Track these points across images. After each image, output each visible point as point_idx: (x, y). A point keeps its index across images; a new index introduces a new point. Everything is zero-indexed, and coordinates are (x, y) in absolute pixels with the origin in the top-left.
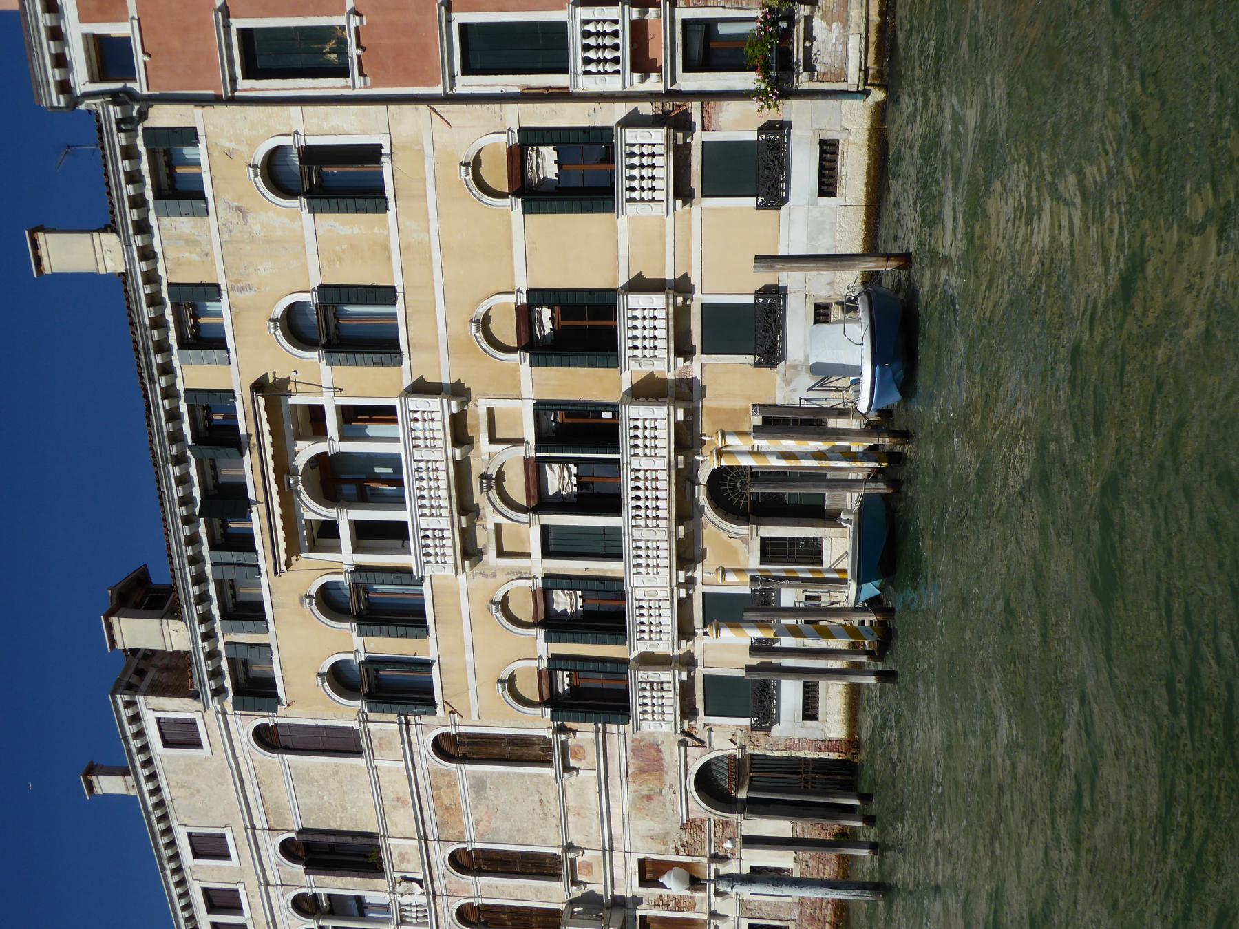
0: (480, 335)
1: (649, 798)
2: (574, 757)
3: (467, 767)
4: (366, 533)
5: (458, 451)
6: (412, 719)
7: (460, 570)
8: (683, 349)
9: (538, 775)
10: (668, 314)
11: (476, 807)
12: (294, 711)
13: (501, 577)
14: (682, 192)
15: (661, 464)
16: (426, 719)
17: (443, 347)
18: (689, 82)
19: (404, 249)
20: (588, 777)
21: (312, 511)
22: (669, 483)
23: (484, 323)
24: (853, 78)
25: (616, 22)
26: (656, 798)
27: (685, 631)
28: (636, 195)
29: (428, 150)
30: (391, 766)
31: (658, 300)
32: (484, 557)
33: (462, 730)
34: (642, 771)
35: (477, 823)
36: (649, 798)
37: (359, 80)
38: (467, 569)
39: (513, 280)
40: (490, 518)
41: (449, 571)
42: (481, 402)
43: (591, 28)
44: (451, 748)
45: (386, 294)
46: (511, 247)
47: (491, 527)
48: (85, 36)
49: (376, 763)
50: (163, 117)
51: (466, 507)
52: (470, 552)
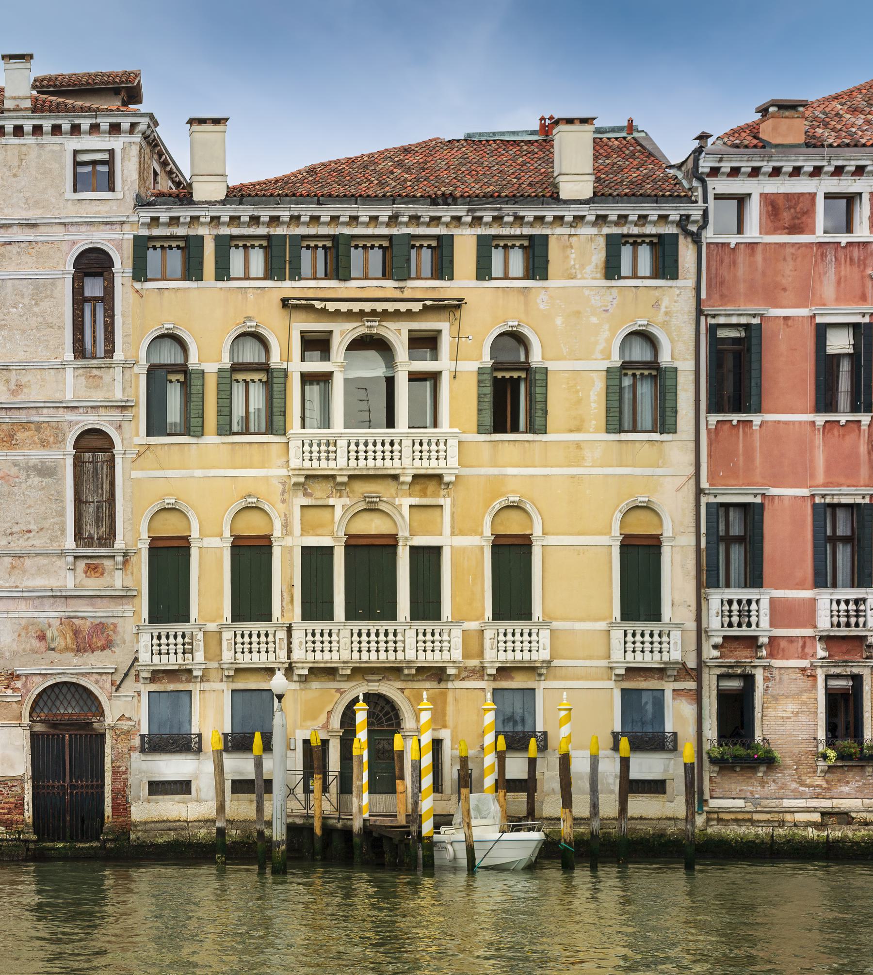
1: (42, 637)
2: (88, 566)
3: (70, 461)
8: (504, 671)
9: (63, 531)
10: (535, 661)
11: (15, 465)
12: (132, 297)
14: (632, 672)
15: (411, 655)
19: (578, 445)
20: (68, 580)
22: (394, 662)
25: (757, 625)
26: (43, 645)
28: (630, 638)
29: (659, 471)
30: (70, 385)
33: (118, 461)
34: (76, 632)
36: (42, 637)
43: (754, 606)
44: (94, 445)
47: (331, 501)
49: (69, 371)
50: (687, 254)
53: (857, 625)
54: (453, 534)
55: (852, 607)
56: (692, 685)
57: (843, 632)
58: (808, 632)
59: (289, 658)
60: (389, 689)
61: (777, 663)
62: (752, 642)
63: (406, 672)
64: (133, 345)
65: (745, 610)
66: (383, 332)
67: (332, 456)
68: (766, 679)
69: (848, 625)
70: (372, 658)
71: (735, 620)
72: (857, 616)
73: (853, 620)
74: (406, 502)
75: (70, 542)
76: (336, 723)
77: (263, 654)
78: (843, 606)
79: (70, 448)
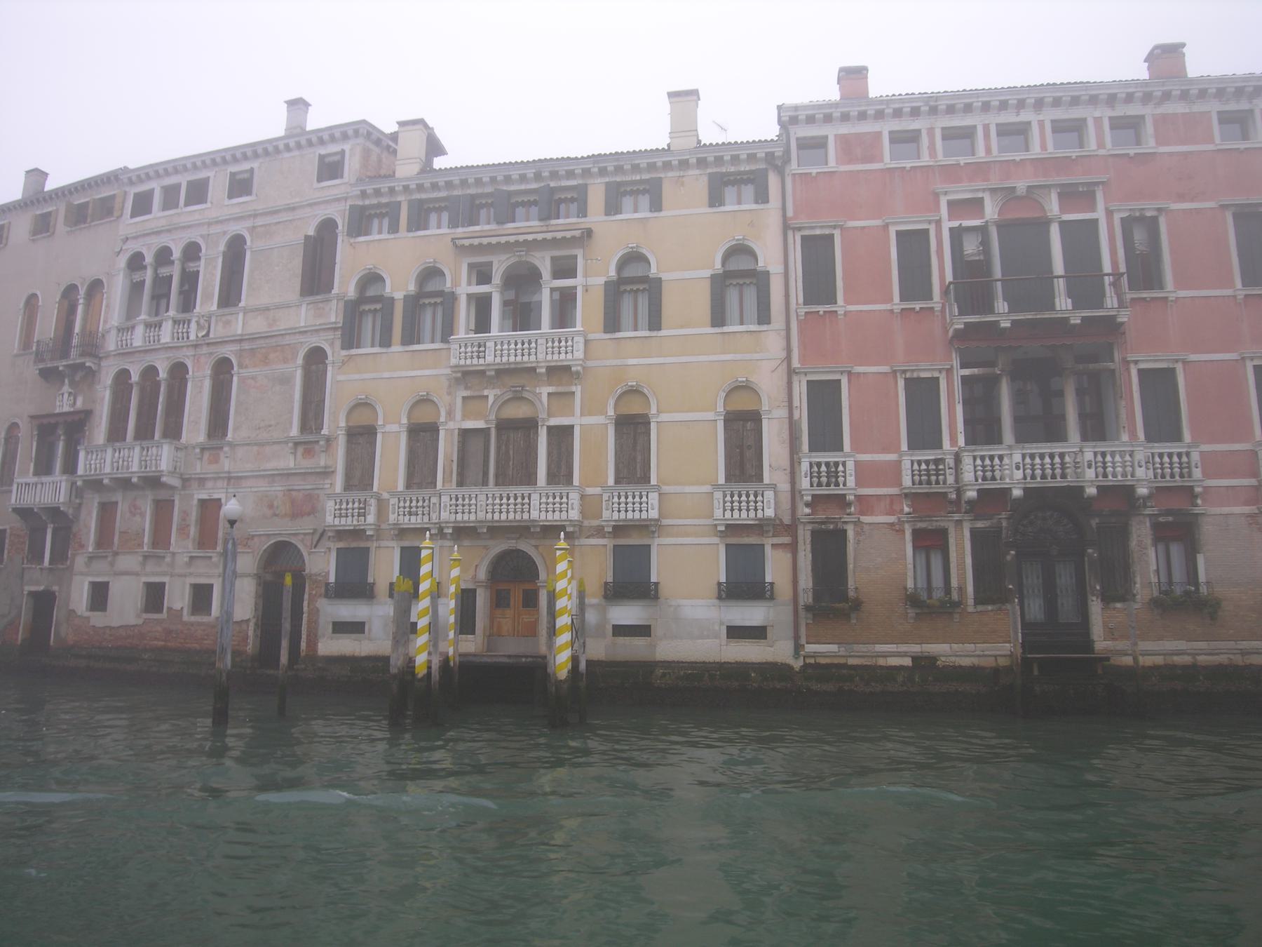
1: (271, 506)
3: (299, 374)
4: (482, 305)
5: (544, 370)
6: (339, 333)
9: (291, 423)
14: (733, 529)
15: (535, 515)
16: (338, 343)
17: (618, 362)
18: (804, 535)
20: (288, 461)
21: (500, 265)
24: (810, 648)
25: (845, 484)
27: (402, 532)
28: (728, 498)
29: (756, 356)
30: (303, 316)
33: (329, 368)
35: (253, 378)
36: (271, 506)
37: (802, 311)
40: (491, 394)
41: (454, 361)
42: (579, 388)
43: (841, 468)
44: (316, 357)
45: (655, 323)
48: (826, 137)
50: (773, 181)
53: (937, 482)
54: (582, 415)
55: (932, 467)
56: (786, 540)
57: (924, 489)
58: (893, 491)
61: (866, 519)
62: (840, 501)
64: (345, 284)
65: (833, 473)
66: (530, 259)
68: (857, 534)
69: (929, 482)
71: (824, 480)
72: (937, 475)
73: (933, 478)
74: (545, 390)
75: (295, 431)
78: (924, 466)
79: (300, 361)
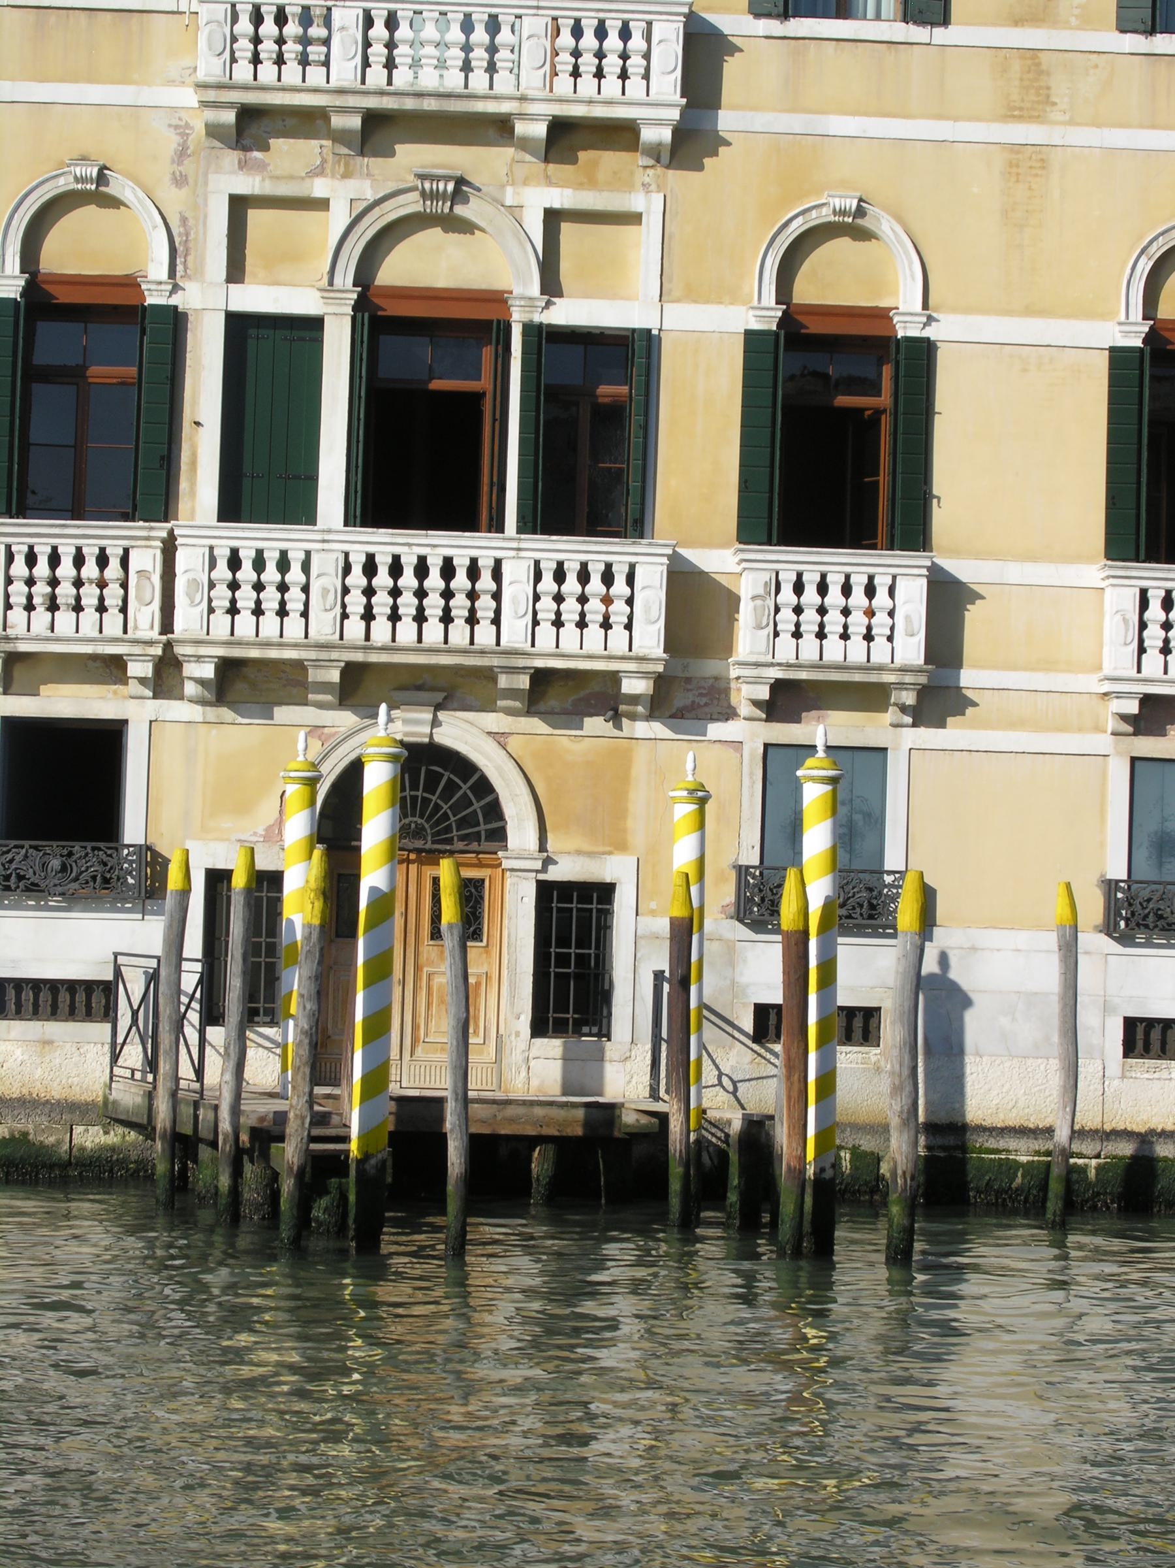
0: (825, 216)
7: (211, 95)
8: (788, 699)
10: (880, 668)
13: (174, 200)
15: (514, 632)
22: (464, 652)
23: (852, 227)
31: (911, 649)
32: (232, 157)
38: (211, 115)
39: (955, 310)
41: (210, 67)
42: (657, 200)
46: (1030, 311)
47: (319, 188)
51: (379, 130)
52: (252, 126)
59: (167, 625)
60: (463, 733)
63: (503, 681)
67: (316, 52)
70: (400, 640)
76: (298, 826)
77: (89, 616)
